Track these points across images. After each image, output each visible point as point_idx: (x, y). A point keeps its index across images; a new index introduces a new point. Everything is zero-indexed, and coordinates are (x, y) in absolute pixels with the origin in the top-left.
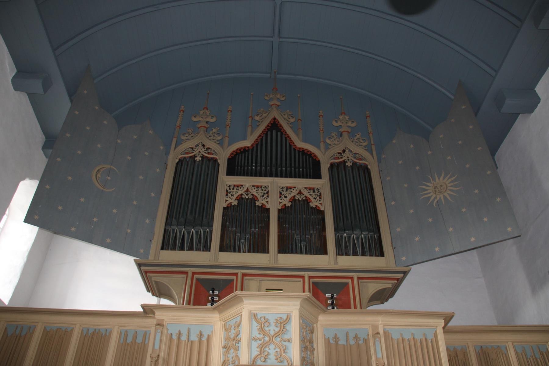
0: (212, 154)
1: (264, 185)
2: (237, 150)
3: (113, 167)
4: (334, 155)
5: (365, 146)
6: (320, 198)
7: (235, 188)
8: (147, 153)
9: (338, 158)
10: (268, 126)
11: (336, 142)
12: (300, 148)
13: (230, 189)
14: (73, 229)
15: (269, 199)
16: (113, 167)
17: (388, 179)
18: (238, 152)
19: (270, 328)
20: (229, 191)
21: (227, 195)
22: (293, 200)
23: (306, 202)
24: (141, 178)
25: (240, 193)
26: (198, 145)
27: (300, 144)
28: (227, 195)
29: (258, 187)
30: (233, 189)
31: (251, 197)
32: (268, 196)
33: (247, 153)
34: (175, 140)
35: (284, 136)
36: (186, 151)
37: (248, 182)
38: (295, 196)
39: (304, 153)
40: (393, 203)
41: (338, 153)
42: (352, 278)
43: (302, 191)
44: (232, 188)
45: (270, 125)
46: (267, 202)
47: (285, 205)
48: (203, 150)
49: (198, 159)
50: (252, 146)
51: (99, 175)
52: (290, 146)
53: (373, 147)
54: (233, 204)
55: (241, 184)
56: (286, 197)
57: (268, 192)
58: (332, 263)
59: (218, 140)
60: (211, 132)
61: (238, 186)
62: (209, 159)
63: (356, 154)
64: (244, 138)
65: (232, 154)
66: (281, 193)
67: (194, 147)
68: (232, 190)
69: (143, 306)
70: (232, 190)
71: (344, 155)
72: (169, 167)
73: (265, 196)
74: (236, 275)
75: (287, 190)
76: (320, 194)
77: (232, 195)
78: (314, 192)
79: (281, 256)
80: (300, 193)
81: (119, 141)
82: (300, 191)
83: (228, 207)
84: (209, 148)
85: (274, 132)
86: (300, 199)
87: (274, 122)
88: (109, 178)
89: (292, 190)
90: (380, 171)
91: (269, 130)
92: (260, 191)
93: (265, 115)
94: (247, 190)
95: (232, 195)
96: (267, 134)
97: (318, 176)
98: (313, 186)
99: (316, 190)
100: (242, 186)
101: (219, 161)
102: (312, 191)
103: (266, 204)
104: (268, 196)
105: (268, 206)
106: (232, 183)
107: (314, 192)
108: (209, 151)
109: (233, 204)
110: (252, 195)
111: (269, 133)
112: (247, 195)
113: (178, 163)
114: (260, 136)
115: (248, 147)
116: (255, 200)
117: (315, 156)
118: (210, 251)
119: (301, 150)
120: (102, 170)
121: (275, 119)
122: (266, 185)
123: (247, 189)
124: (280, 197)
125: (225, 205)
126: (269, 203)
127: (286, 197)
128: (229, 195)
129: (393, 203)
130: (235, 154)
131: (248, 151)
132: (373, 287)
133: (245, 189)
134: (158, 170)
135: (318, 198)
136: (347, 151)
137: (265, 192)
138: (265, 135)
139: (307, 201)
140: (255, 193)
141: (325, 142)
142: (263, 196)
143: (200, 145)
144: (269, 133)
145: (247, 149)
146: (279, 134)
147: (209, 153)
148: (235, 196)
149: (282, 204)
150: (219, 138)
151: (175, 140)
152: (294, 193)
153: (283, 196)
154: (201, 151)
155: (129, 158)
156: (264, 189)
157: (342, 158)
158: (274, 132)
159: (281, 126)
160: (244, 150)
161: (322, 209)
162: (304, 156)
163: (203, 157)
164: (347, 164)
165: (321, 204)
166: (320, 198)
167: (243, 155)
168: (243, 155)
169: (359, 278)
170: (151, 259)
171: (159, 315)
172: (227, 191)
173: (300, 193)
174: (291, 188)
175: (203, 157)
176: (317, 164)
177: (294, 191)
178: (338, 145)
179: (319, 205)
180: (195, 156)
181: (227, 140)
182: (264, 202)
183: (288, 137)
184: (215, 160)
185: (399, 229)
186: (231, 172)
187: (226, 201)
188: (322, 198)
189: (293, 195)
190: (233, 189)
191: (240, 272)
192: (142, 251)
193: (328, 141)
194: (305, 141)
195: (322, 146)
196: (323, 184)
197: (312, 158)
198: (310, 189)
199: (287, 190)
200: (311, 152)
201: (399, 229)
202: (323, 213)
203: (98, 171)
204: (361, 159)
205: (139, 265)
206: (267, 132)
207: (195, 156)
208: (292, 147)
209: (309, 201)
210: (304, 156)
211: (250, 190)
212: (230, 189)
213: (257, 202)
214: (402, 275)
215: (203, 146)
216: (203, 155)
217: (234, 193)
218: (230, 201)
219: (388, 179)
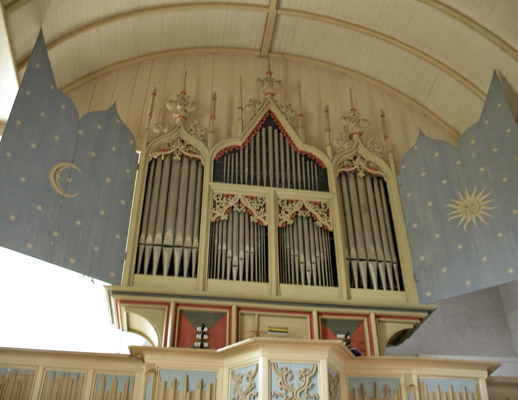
0: (195, 153)
1: (260, 196)
2: (225, 149)
3: (74, 166)
4: (343, 162)
5: (380, 153)
6: (328, 216)
7: (224, 199)
8: (114, 149)
9: (349, 166)
10: (262, 121)
11: (346, 146)
12: (302, 152)
13: (218, 199)
14: (30, 246)
15: (266, 215)
16: (74, 166)
17: (409, 195)
18: (227, 152)
19: (293, 381)
20: (217, 202)
21: (214, 206)
22: (295, 216)
23: (310, 220)
24: (108, 180)
25: (231, 204)
28: (214, 206)
29: (252, 198)
30: (222, 199)
31: (244, 210)
32: (265, 211)
33: (237, 154)
35: (281, 134)
36: (162, 148)
37: (241, 191)
38: (297, 212)
39: (308, 157)
40: (415, 226)
41: (348, 160)
42: (368, 316)
43: (306, 206)
44: (220, 198)
45: (265, 120)
46: (264, 218)
47: (286, 222)
48: (183, 147)
50: (243, 145)
51: (58, 176)
52: (290, 148)
54: (222, 219)
55: (232, 193)
56: (287, 213)
57: (264, 206)
58: (345, 296)
59: (201, 136)
60: (192, 125)
61: (227, 196)
62: (190, 160)
63: (368, 162)
65: (219, 154)
66: (280, 208)
67: (171, 143)
68: (220, 201)
69: (131, 348)
70: (220, 201)
71: (356, 163)
72: (141, 167)
73: (261, 210)
74: (230, 308)
75: (288, 204)
76: (328, 210)
77: (221, 207)
78: (320, 207)
79: (284, 287)
80: (304, 208)
81: (80, 132)
82: (304, 206)
83: (215, 222)
84: (190, 146)
85: (270, 129)
86: (304, 216)
87: (270, 116)
88: (70, 180)
89: (294, 204)
90: (399, 185)
91: (263, 126)
92: (255, 204)
95: (221, 207)
96: (261, 131)
97: (324, 187)
98: (318, 201)
99: (323, 206)
100: (233, 196)
101: (203, 162)
102: (318, 207)
103: (263, 220)
104: (265, 211)
105: (265, 223)
106: (220, 192)
107: (320, 207)
108: (191, 148)
109: (222, 219)
110: (246, 208)
111: (264, 130)
112: (240, 208)
113: (150, 164)
114: (253, 133)
115: (239, 147)
116: (249, 216)
117: (320, 162)
118: (196, 276)
119: (304, 154)
120: (61, 170)
121: (270, 112)
122: (262, 196)
123: (239, 201)
124: (280, 212)
125: (213, 219)
126: (267, 219)
127: (287, 213)
128: (218, 207)
129: (415, 226)
130: (222, 154)
132: (392, 329)
133: (237, 201)
134: (128, 171)
135: (326, 215)
136: (359, 157)
137: (262, 205)
138: (258, 133)
139: (312, 219)
140: (249, 207)
142: (259, 210)
143: (179, 141)
144: (264, 130)
145: (237, 149)
146: (276, 131)
147: (189, 151)
148: (225, 209)
149: (282, 222)
150: (203, 133)
152: (297, 207)
153: (283, 212)
154: (180, 148)
155: (93, 154)
156: (260, 201)
157: (353, 166)
158: (270, 129)
159: (278, 122)
161: (330, 229)
162: (308, 162)
163: (182, 156)
164: (359, 175)
165: (329, 223)
166: (328, 216)
167: (233, 155)
168: (233, 155)
169: (377, 316)
170: (123, 287)
171: (149, 358)
172: (214, 202)
174: (292, 202)
175: (182, 156)
176: (323, 172)
177: (297, 206)
178: (348, 150)
179: (328, 225)
180: (172, 155)
182: (261, 218)
183: (287, 136)
184: (198, 161)
185: (422, 258)
186: (217, 177)
187: (214, 214)
188: (331, 216)
189: (295, 210)
190: (222, 199)
191: (234, 305)
192: (112, 275)
196: (331, 197)
197: (318, 165)
198: (316, 204)
199: (288, 204)
200: (315, 157)
201: (422, 258)
202: (331, 234)
203: (57, 170)
204: (376, 170)
206: (261, 129)
207: (172, 155)
209: (314, 219)
210: (308, 162)
211: (242, 201)
212: (218, 199)
213: (251, 217)
214: (426, 314)
215: (183, 141)
216: (183, 155)
217: (223, 205)
218: (218, 214)
219: (409, 195)
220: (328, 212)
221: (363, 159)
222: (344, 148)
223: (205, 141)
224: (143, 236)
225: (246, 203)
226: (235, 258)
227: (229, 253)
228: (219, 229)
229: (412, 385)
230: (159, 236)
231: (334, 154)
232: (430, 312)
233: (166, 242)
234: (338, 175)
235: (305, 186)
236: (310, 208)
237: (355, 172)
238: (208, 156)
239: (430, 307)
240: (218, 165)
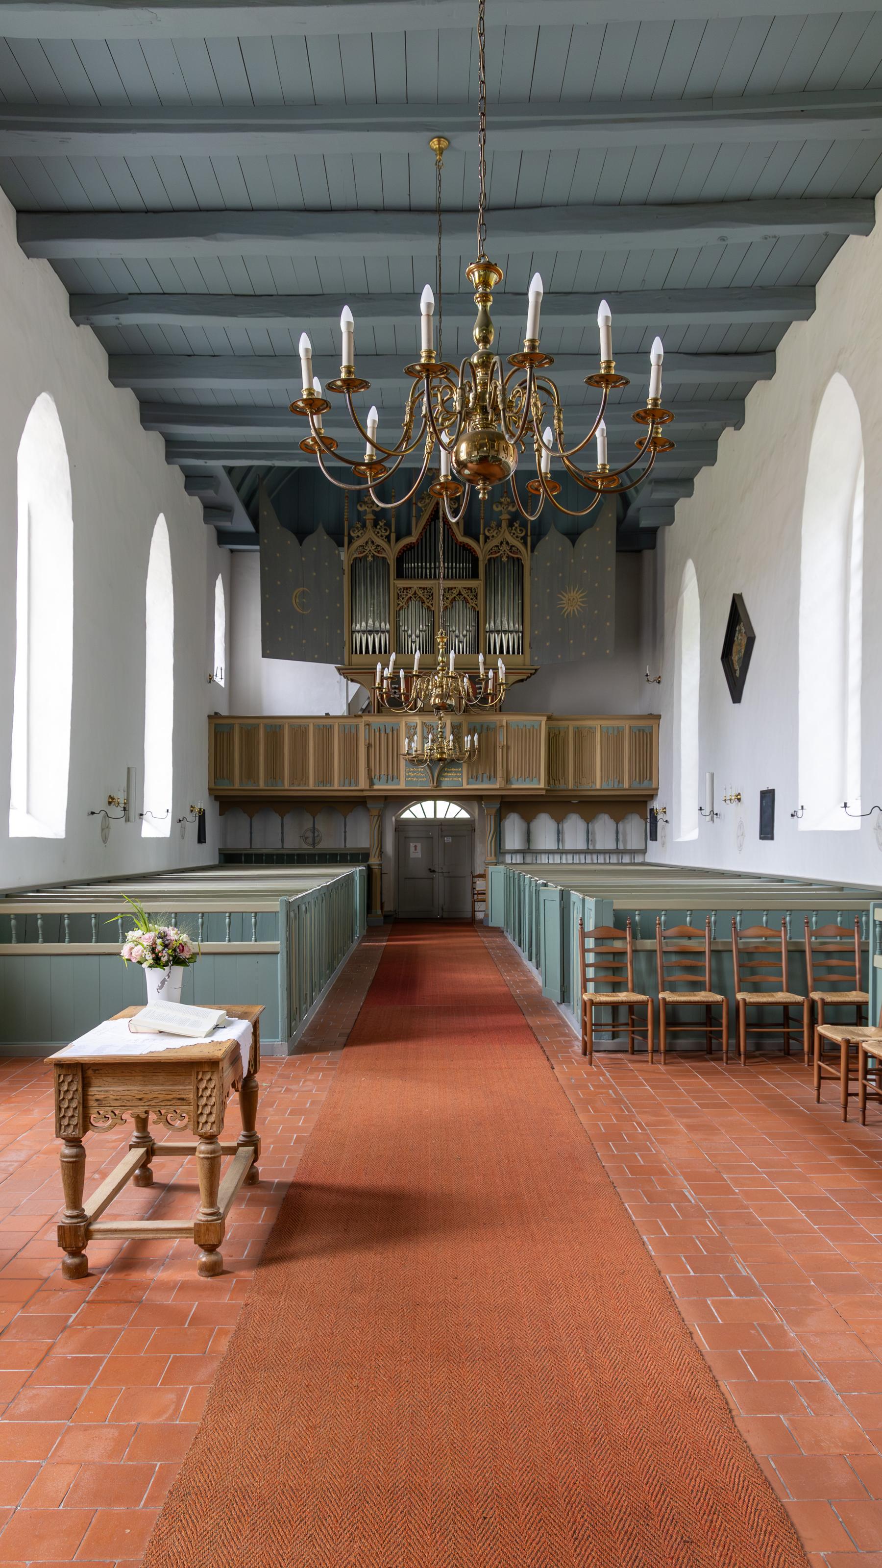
9: (496, 552)
11: (494, 534)
25: (409, 595)
26: (367, 543)
27: (461, 539)
29: (424, 589)
34: (346, 539)
37: (415, 584)
39: (465, 547)
49: (370, 559)
53: (529, 539)
61: (407, 589)
63: (512, 546)
64: (409, 533)
80: (460, 594)
84: (378, 546)
90: (531, 569)
93: (427, 501)
94: (415, 593)
96: (430, 525)
97: (475, 575)
106: (401, 586)
114: (424, 528)
131: (414, 548)
141: (484, 534)
150: (387, 534)
151: (346, 539)
160: (409, 547)
173: (460, 594)
174: (452, 589)
176: (475, 560)
181: (393, 536)
186: (400, 575)
193: (487, 534)
194: (467, 533)
195: (482, 538)
198: (468, 589)
204: (517, 553)
205: (339, 669)
208: (454, 541)
215: (373, 542)
220: (476, 596)
221: (507, 543)
222: (493, 536)
223: (388, 538)
224: (354, 626)
225: (420, 593)
226: (414, 636)
227: (410, 632)
228: (402, 613)
229: (502, 726)
230: (364, 624)
231: (486, 542)
232: (536, 670)
233: (369, 628)
234: (486, 562)
235: (461, 577)
236: (464, 592)
237: (501, 557)
238: (392, 557)
239: (536, 667)
240: (400, 560)
